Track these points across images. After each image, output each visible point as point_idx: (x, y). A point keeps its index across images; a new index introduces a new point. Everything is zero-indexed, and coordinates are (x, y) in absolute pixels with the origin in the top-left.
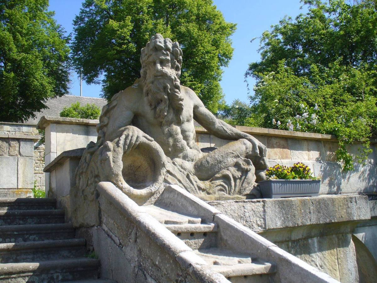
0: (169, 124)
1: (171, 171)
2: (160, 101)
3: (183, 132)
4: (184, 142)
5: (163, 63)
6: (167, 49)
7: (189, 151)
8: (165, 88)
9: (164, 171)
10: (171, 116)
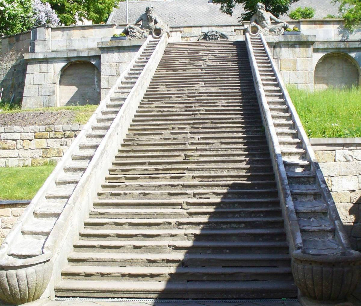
0: (263, 21)
1: (261, 30)
2: (260, 17)
3: (266, 23)
4: (267, 25)
5: (260, 9)
6: (260, 6)
7: (268, 27)
8: (260, 14)
9: (259, 31)
10: (263, 19)
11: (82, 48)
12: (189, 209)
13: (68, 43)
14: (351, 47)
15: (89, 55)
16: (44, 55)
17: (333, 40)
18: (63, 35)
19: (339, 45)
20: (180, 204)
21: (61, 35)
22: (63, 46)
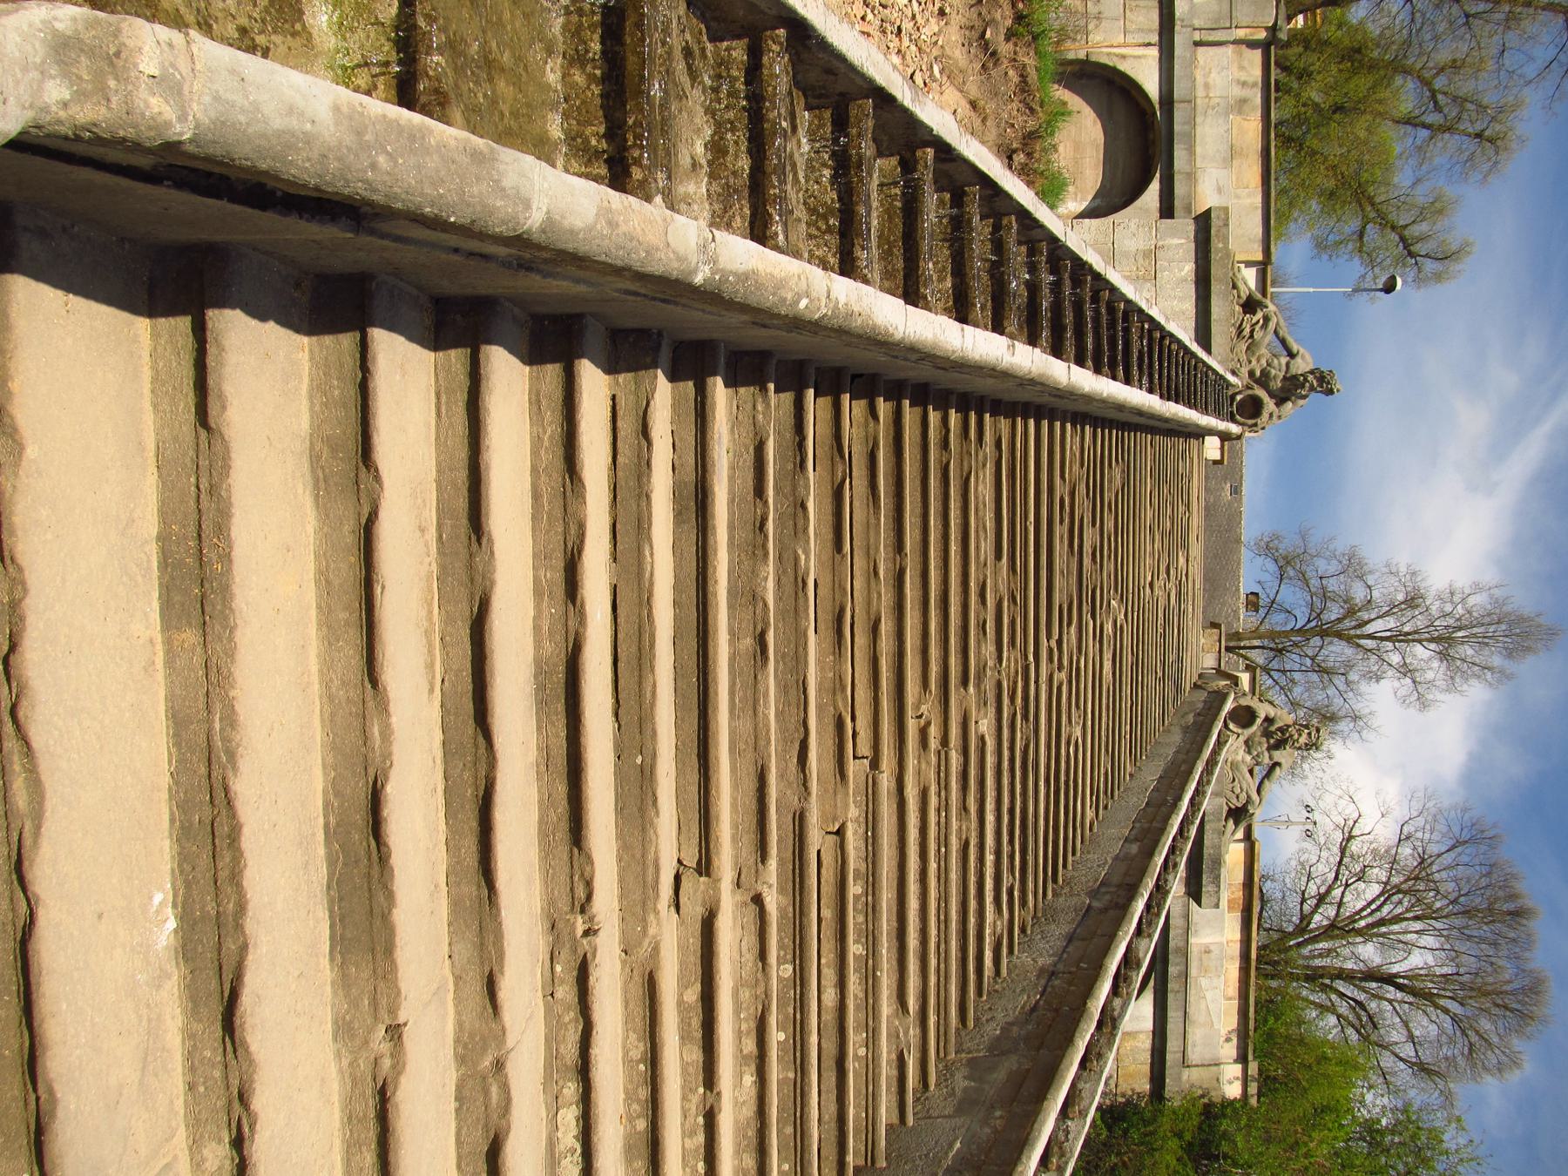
11: (1198, 150)
12: (678, 912)
13: (1217, 100)
14: (1170, 996)
15: (1176, 177)
16: (1183, 21)
17: (1192, 940)
18: (1244, 84)
19: (1178, 960)
20: (705, 867)
21: (1243, 76)
22: (1207, 86)
